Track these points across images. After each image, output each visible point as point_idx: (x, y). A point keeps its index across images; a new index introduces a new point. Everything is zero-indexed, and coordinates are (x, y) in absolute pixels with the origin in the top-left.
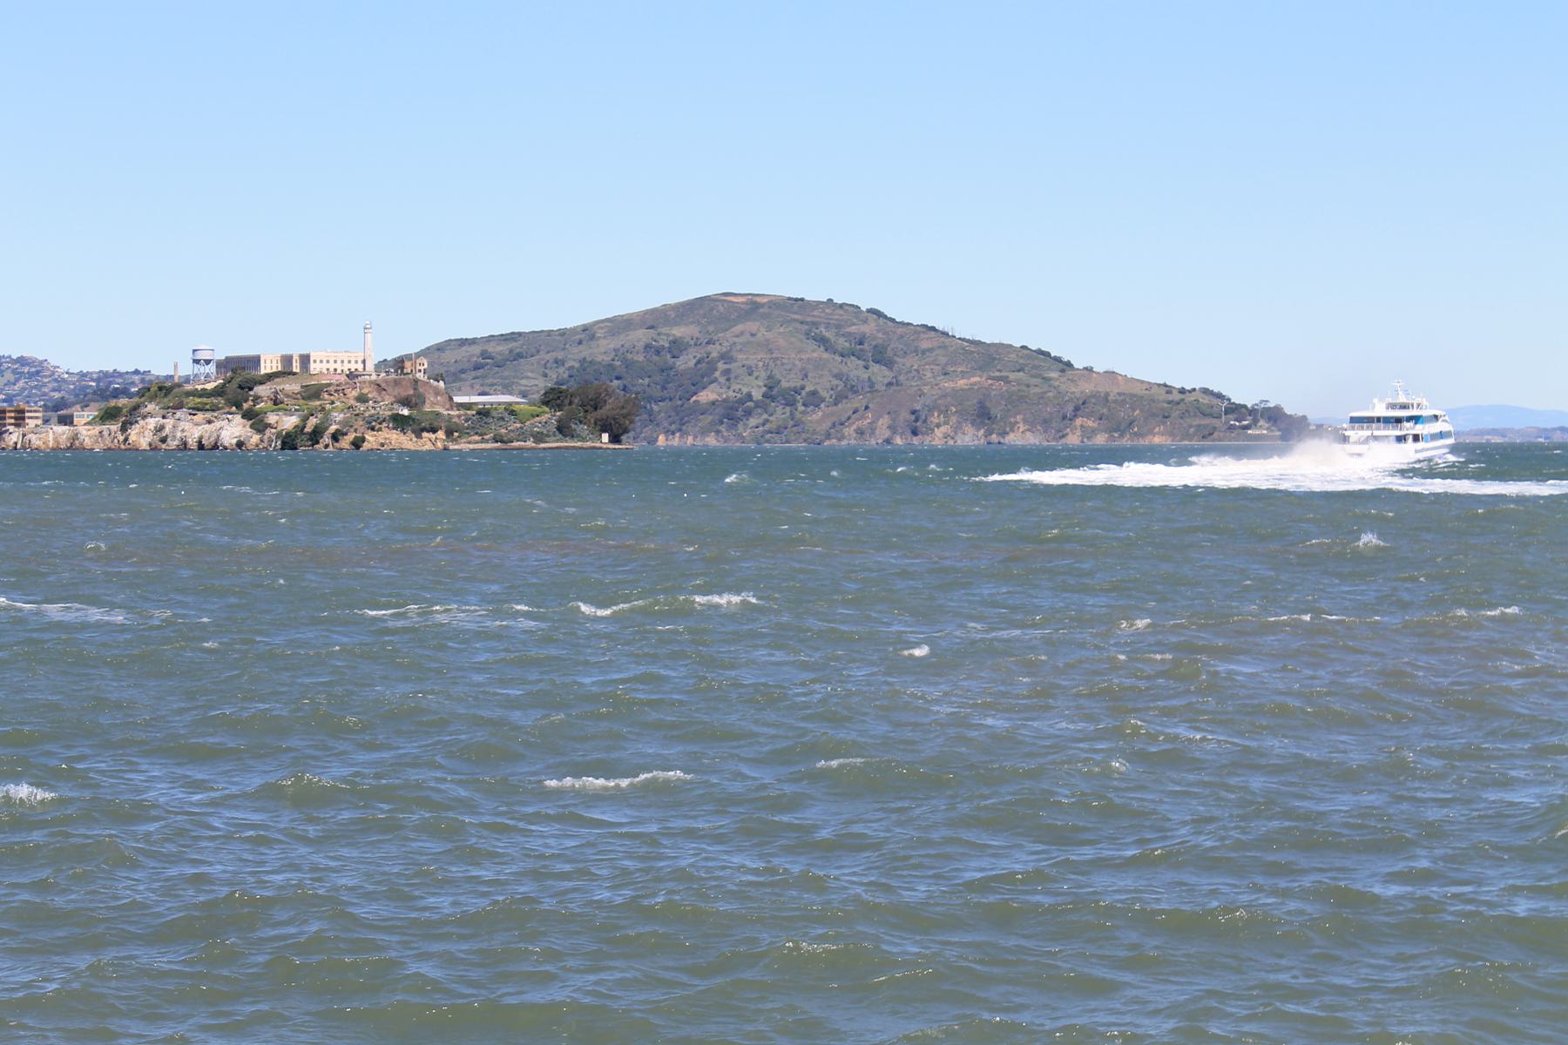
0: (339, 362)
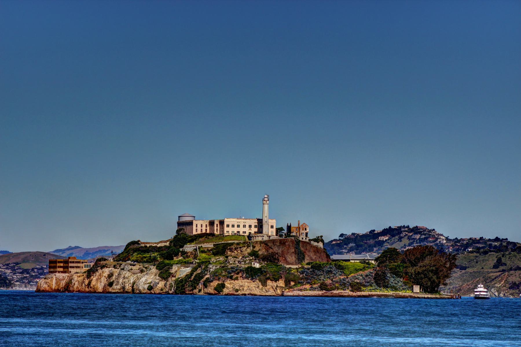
0: (247, 226)
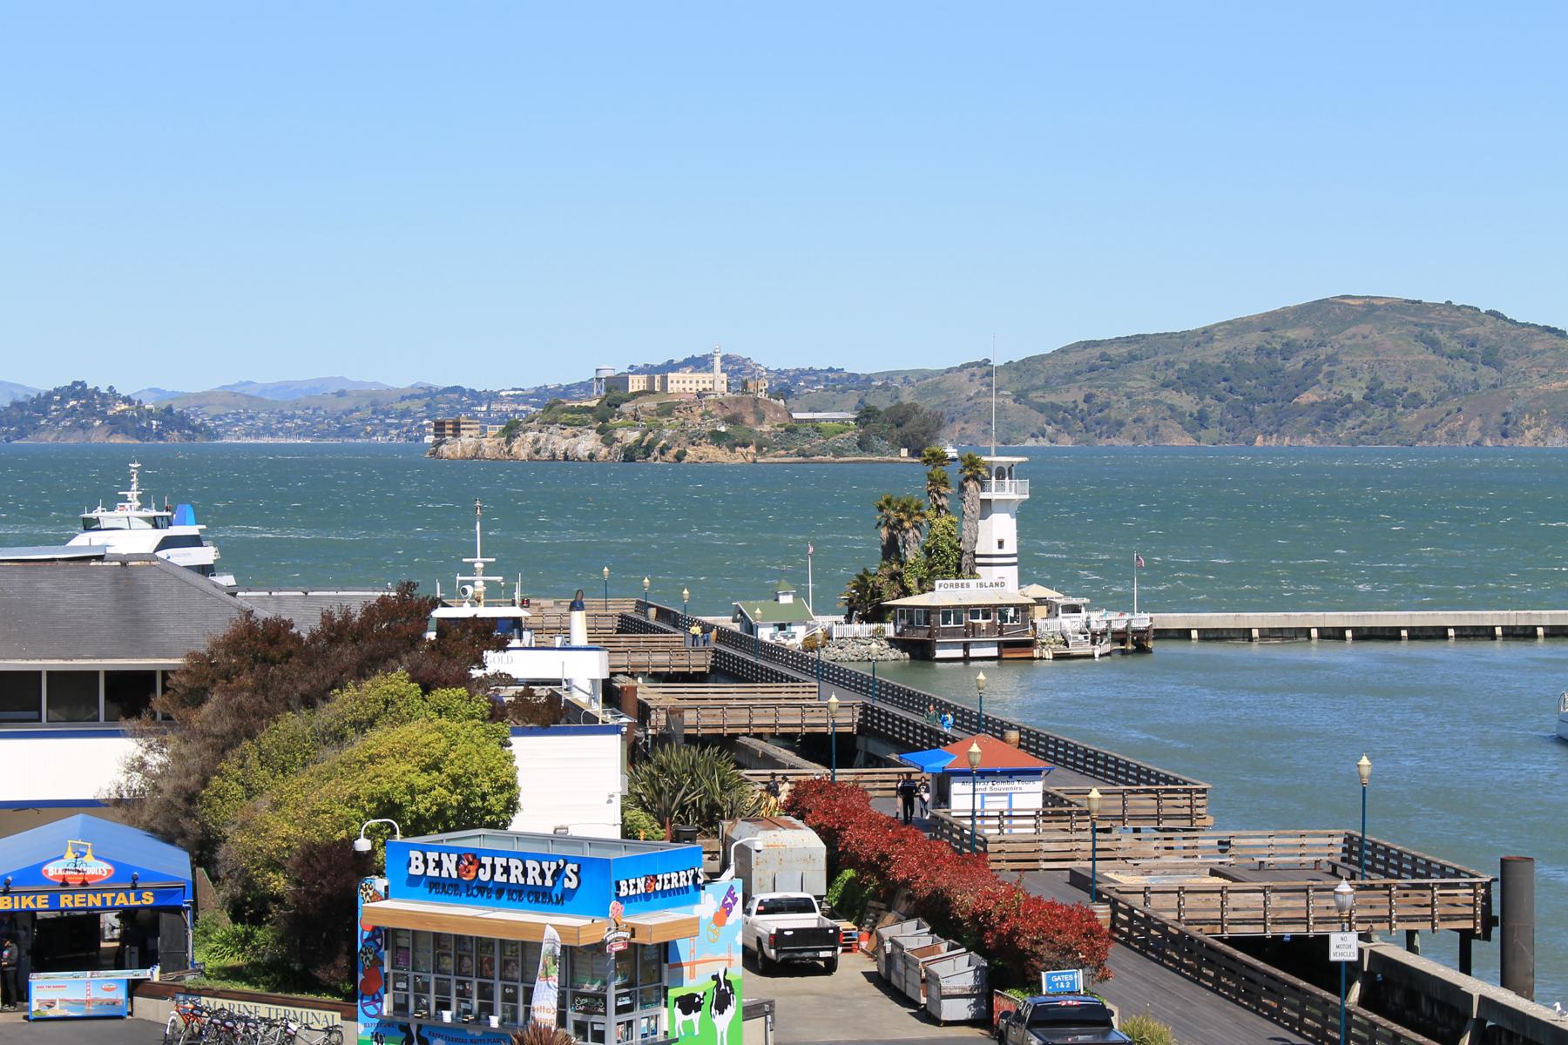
0: (694, 382)
